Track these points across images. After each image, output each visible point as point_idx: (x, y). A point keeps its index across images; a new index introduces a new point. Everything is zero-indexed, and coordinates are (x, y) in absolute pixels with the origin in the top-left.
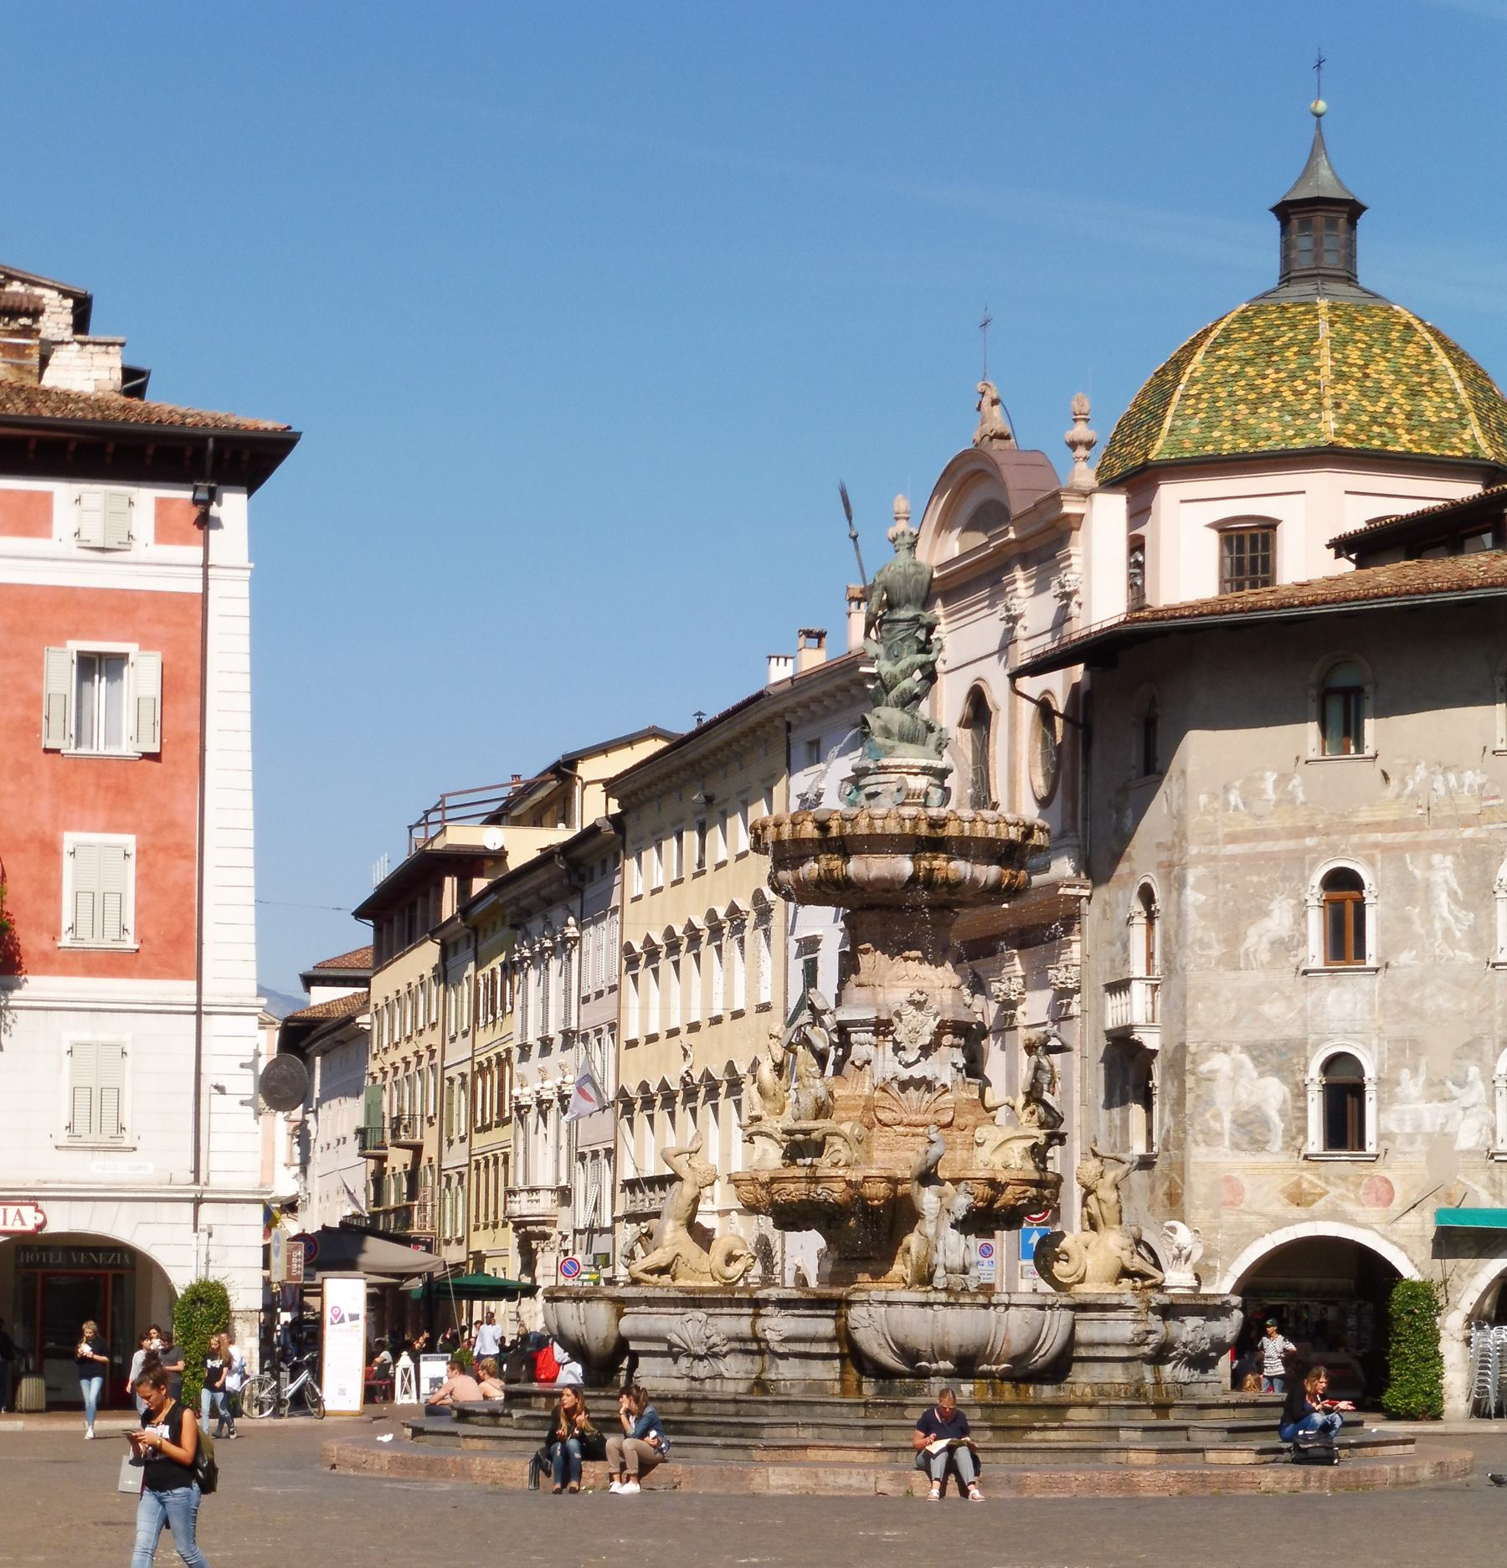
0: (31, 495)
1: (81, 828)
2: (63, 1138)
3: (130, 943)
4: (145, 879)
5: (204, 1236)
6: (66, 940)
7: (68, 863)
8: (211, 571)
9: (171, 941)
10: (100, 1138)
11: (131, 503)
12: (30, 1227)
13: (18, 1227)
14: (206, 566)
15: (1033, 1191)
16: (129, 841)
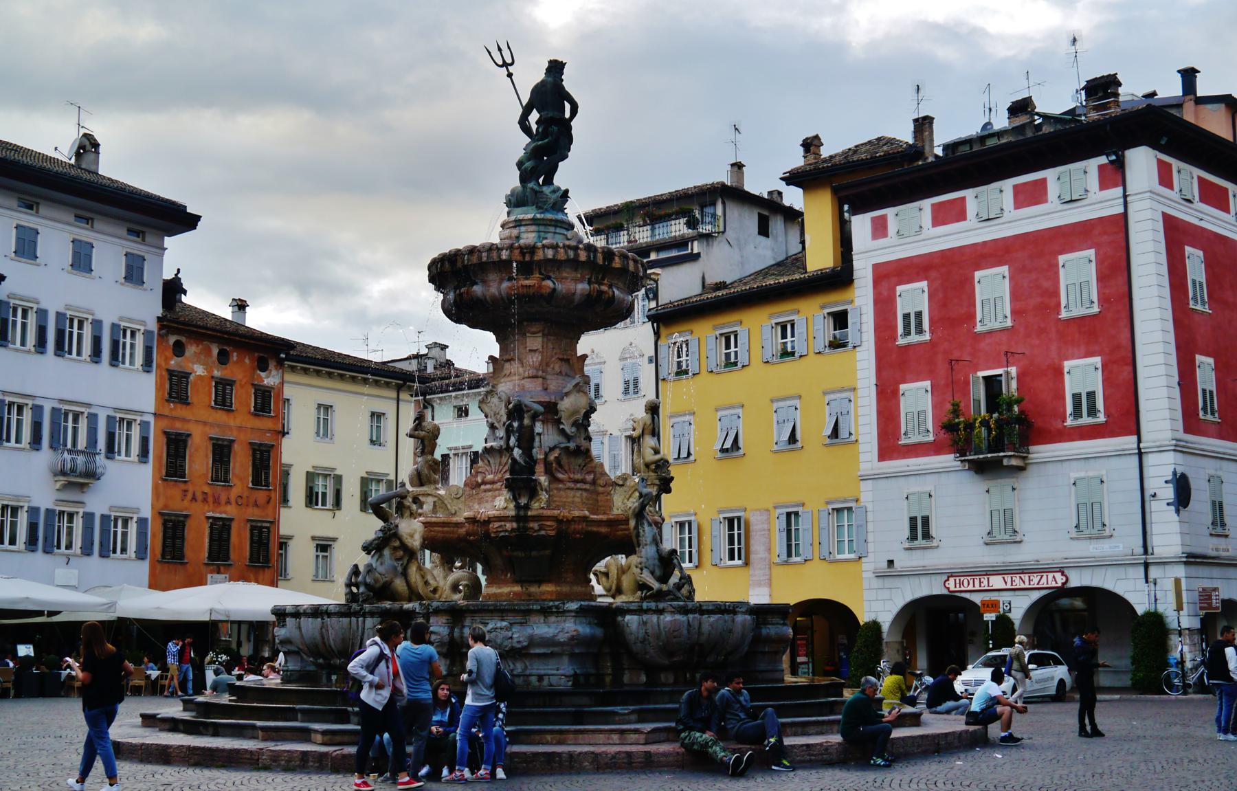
0: (1035, 182)
1: (1073, 358)
2: (1074, 534)
3: (1101, 418)
4: (1106, 381)
5: (1152, 585)
6: (1069, 422)
7: (1067, 377)
8: (1129, 199)
9: (1125, 417)
10: (1093, 531)
11: (1085, 172)
12: (1059, 585)
13: (1054, 585)
14: (1125, 196)
15: (508, 526)
16: (1097, 360)
